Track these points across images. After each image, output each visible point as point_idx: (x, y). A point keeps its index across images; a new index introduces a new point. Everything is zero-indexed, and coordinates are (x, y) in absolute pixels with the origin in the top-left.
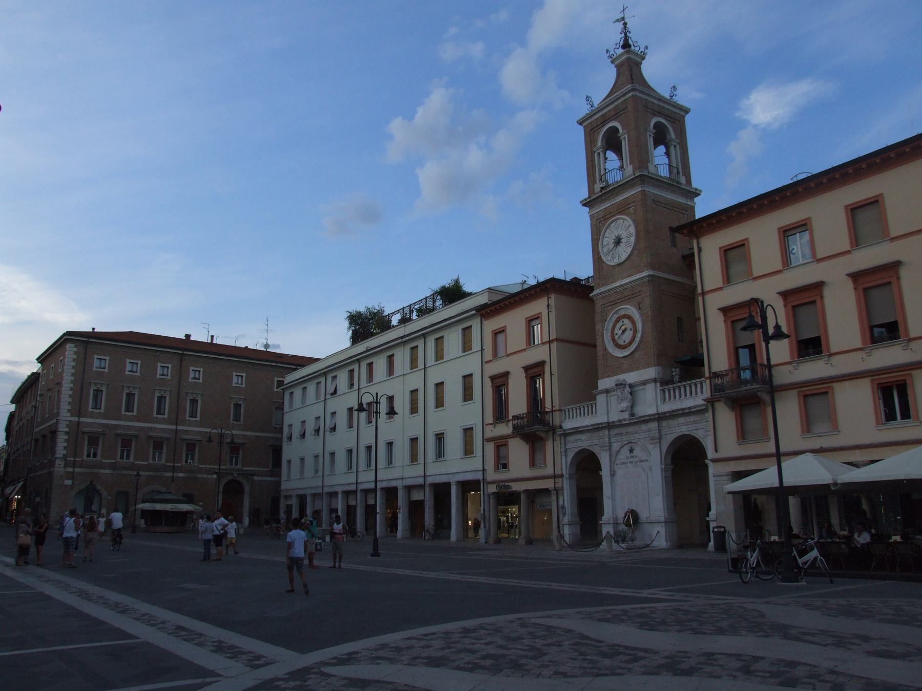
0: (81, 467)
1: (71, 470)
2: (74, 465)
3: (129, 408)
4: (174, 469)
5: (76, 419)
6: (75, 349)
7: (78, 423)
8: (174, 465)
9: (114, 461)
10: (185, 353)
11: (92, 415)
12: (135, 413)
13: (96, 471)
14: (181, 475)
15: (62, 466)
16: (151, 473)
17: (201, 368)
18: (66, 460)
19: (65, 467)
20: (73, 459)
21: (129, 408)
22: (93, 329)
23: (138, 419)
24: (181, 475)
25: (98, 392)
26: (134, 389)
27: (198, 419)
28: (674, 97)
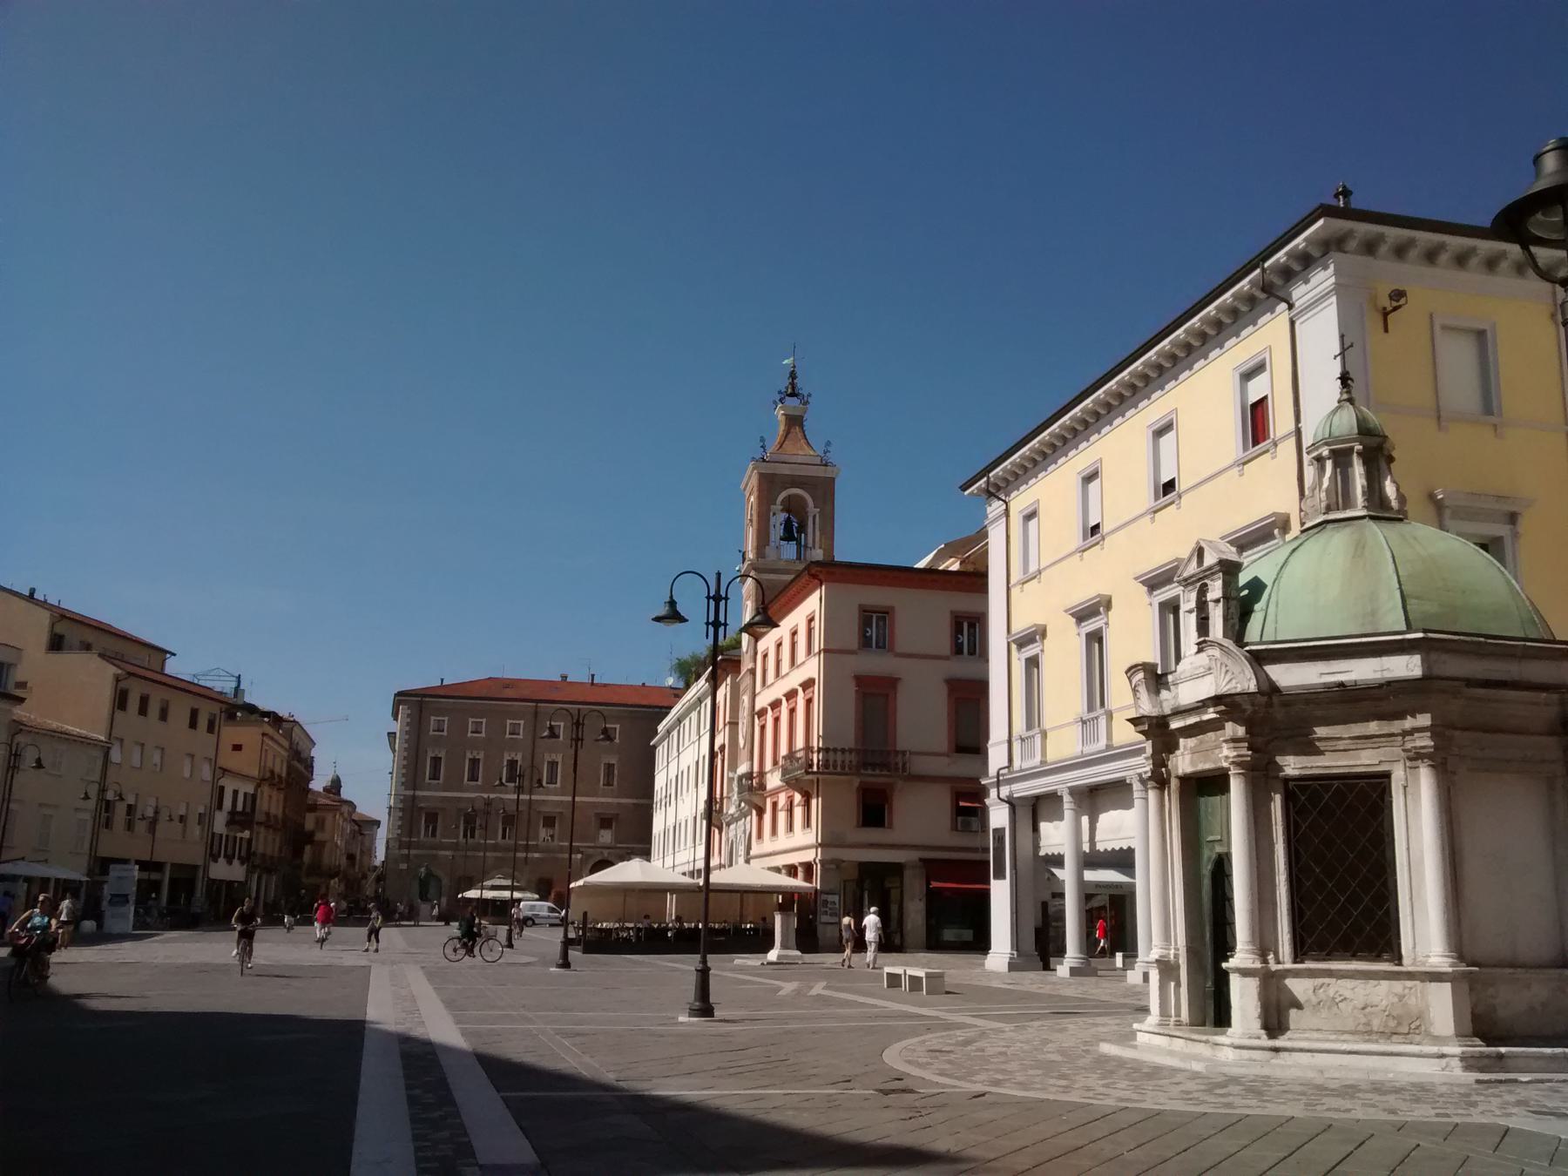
0: (418, 848)
1: (406, 851)
2: (409, 846)
3: (473, 778)
4: (527, 848)
5: (410, 793)
6: (409, 712)
7: (414, 797)
8: (527, 844)
9: (455, 841)
10: (539, 705)
11: (429, 788)
12: (479, 783)
13: (434, 852)
14: (536, 855)
15: (397, 847)
16: (499, 854)
17: (561, 721)
18: (400, 841)
19: (400, 848)
20: (408, 839)
21: (473, 778)
22: (442, 680)
23: (482, 789)
24: (536, 855)
25: (436, 761)
26: (478, 754)
27: (558, 785)
28: (828, 454)
